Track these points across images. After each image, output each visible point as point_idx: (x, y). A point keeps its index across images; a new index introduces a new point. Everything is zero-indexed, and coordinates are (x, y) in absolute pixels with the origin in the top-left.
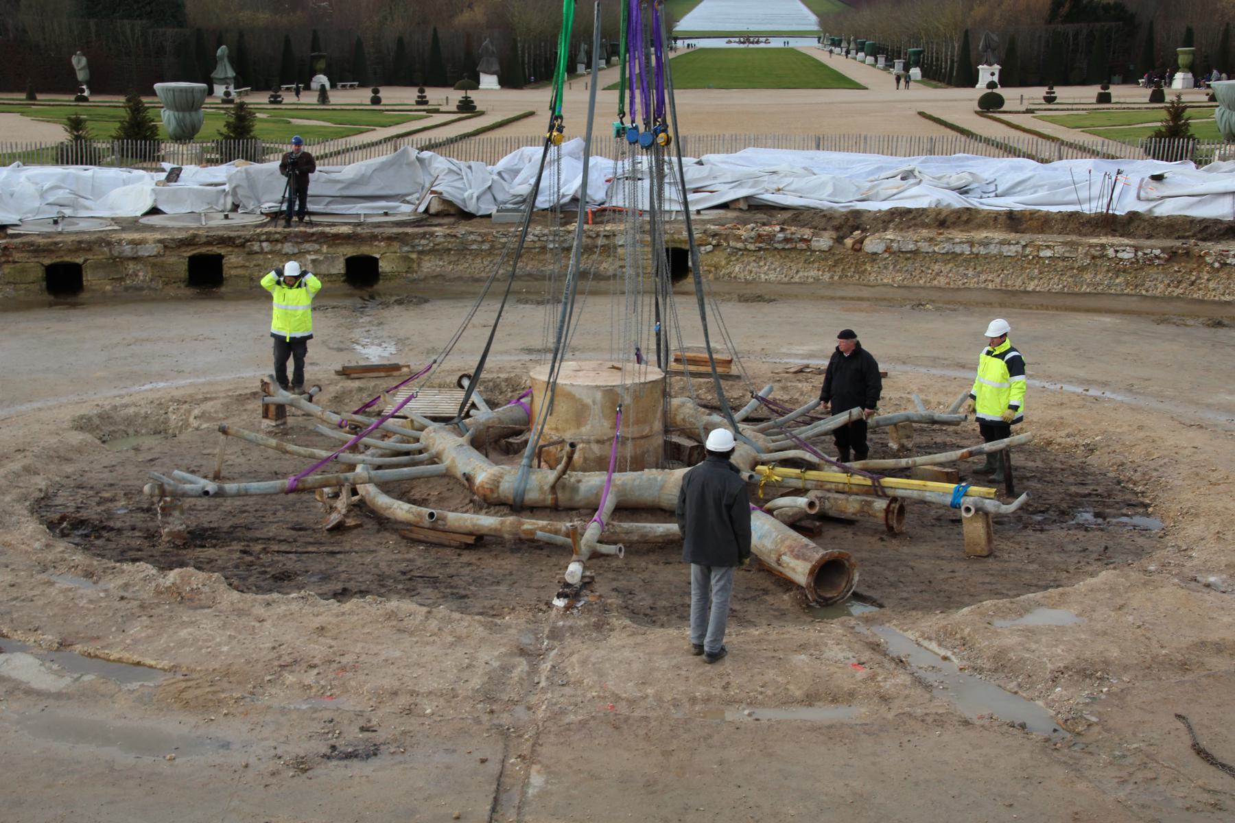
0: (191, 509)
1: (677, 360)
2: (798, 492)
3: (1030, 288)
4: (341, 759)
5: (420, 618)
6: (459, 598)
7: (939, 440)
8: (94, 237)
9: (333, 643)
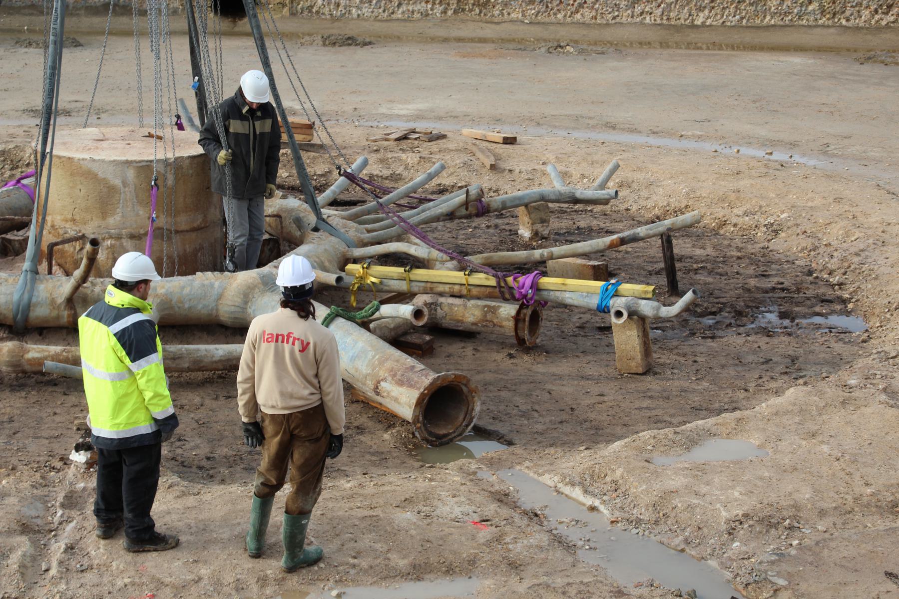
2: (400, 297)
3: (698, 22)
7: (582, 224)
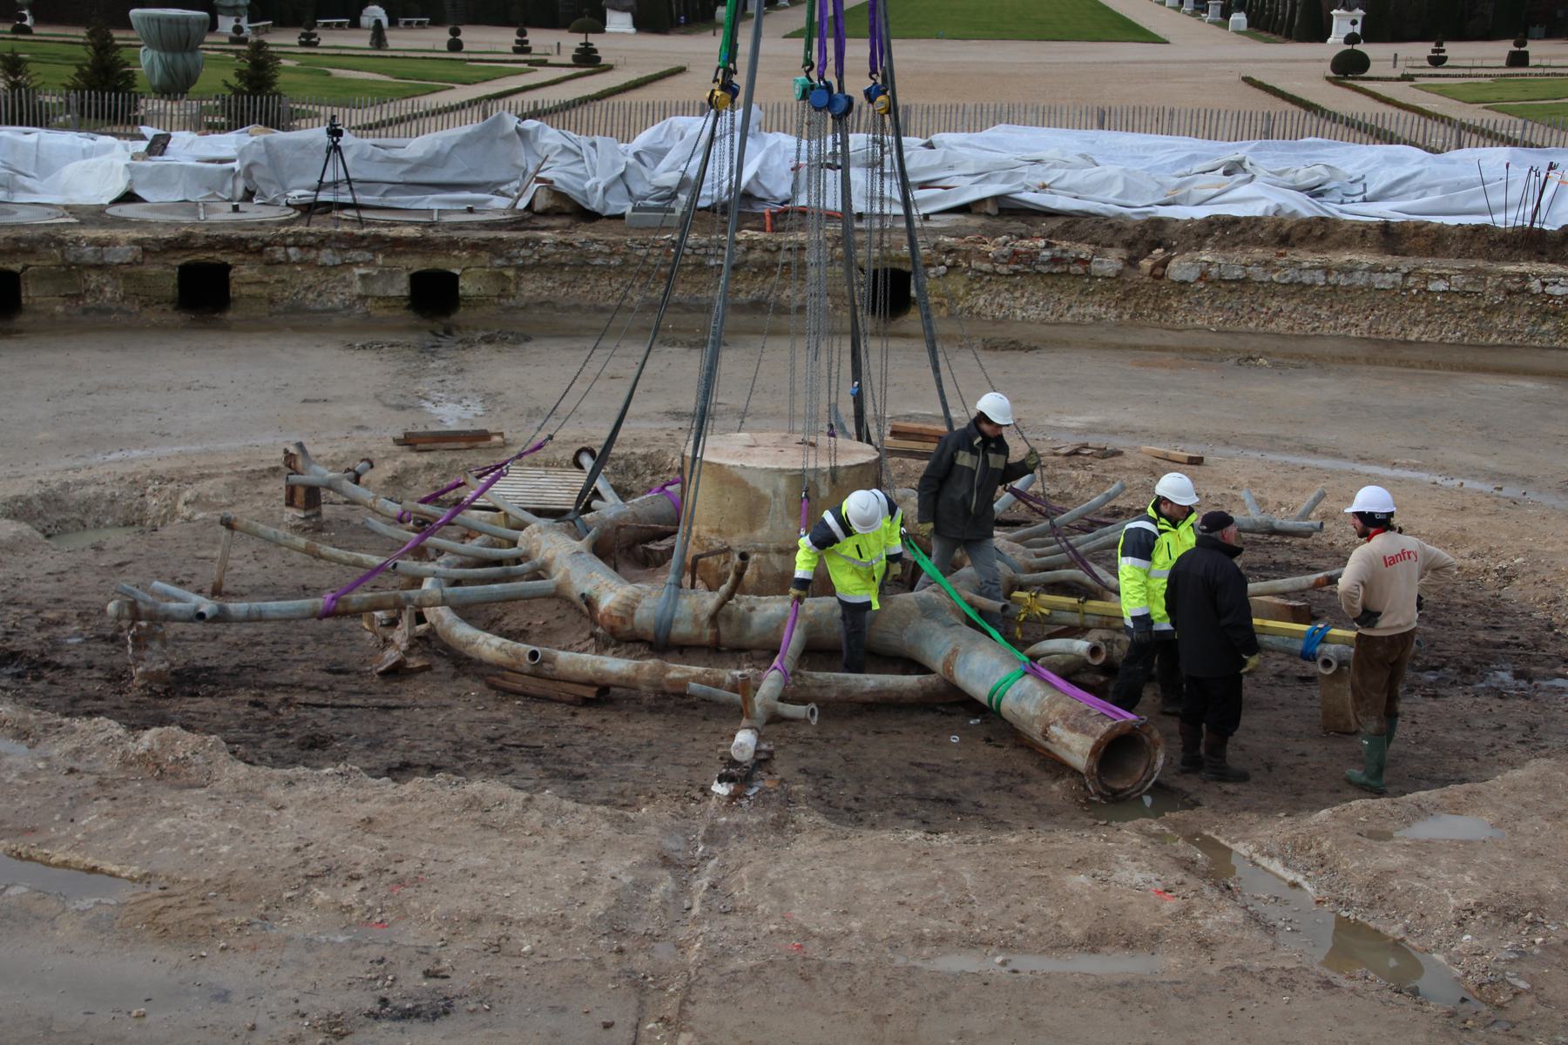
0: (177, 638)
1: (894, 433)
4: (395, 1019)
5: (515, 808)
6: (571, 778)
7: (1279, 558)
8: (38, 233)
9: (386, 843)
